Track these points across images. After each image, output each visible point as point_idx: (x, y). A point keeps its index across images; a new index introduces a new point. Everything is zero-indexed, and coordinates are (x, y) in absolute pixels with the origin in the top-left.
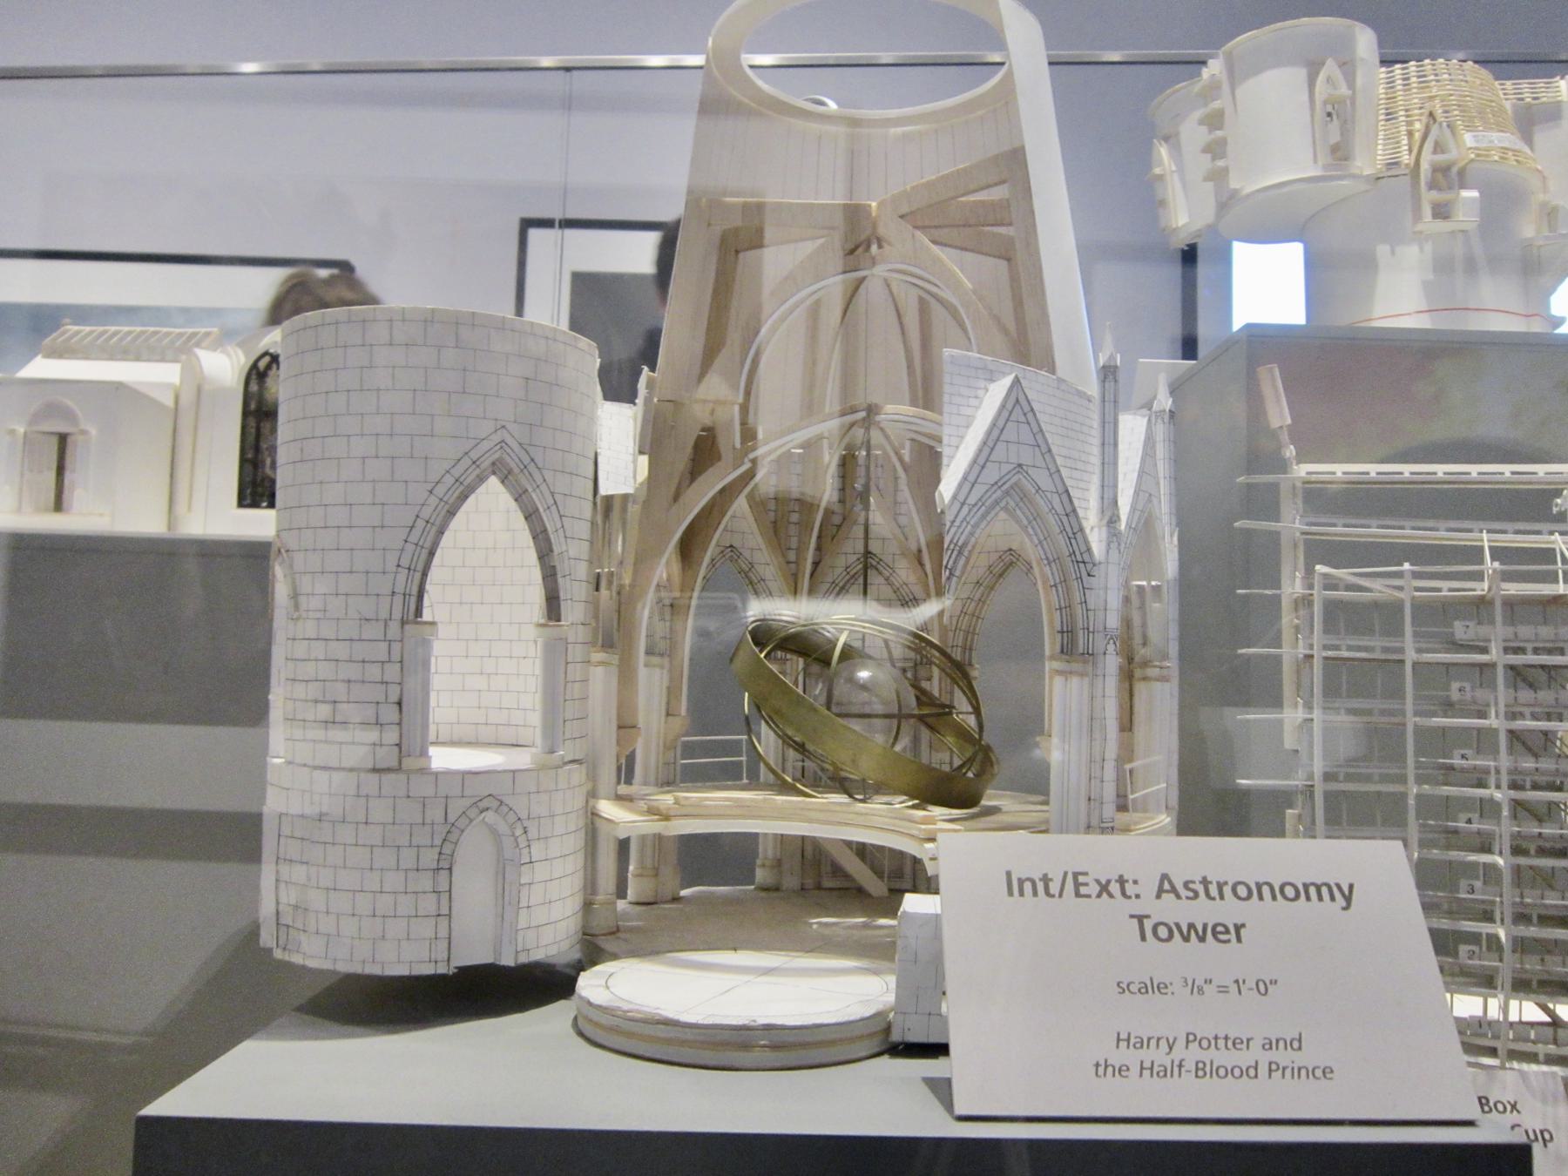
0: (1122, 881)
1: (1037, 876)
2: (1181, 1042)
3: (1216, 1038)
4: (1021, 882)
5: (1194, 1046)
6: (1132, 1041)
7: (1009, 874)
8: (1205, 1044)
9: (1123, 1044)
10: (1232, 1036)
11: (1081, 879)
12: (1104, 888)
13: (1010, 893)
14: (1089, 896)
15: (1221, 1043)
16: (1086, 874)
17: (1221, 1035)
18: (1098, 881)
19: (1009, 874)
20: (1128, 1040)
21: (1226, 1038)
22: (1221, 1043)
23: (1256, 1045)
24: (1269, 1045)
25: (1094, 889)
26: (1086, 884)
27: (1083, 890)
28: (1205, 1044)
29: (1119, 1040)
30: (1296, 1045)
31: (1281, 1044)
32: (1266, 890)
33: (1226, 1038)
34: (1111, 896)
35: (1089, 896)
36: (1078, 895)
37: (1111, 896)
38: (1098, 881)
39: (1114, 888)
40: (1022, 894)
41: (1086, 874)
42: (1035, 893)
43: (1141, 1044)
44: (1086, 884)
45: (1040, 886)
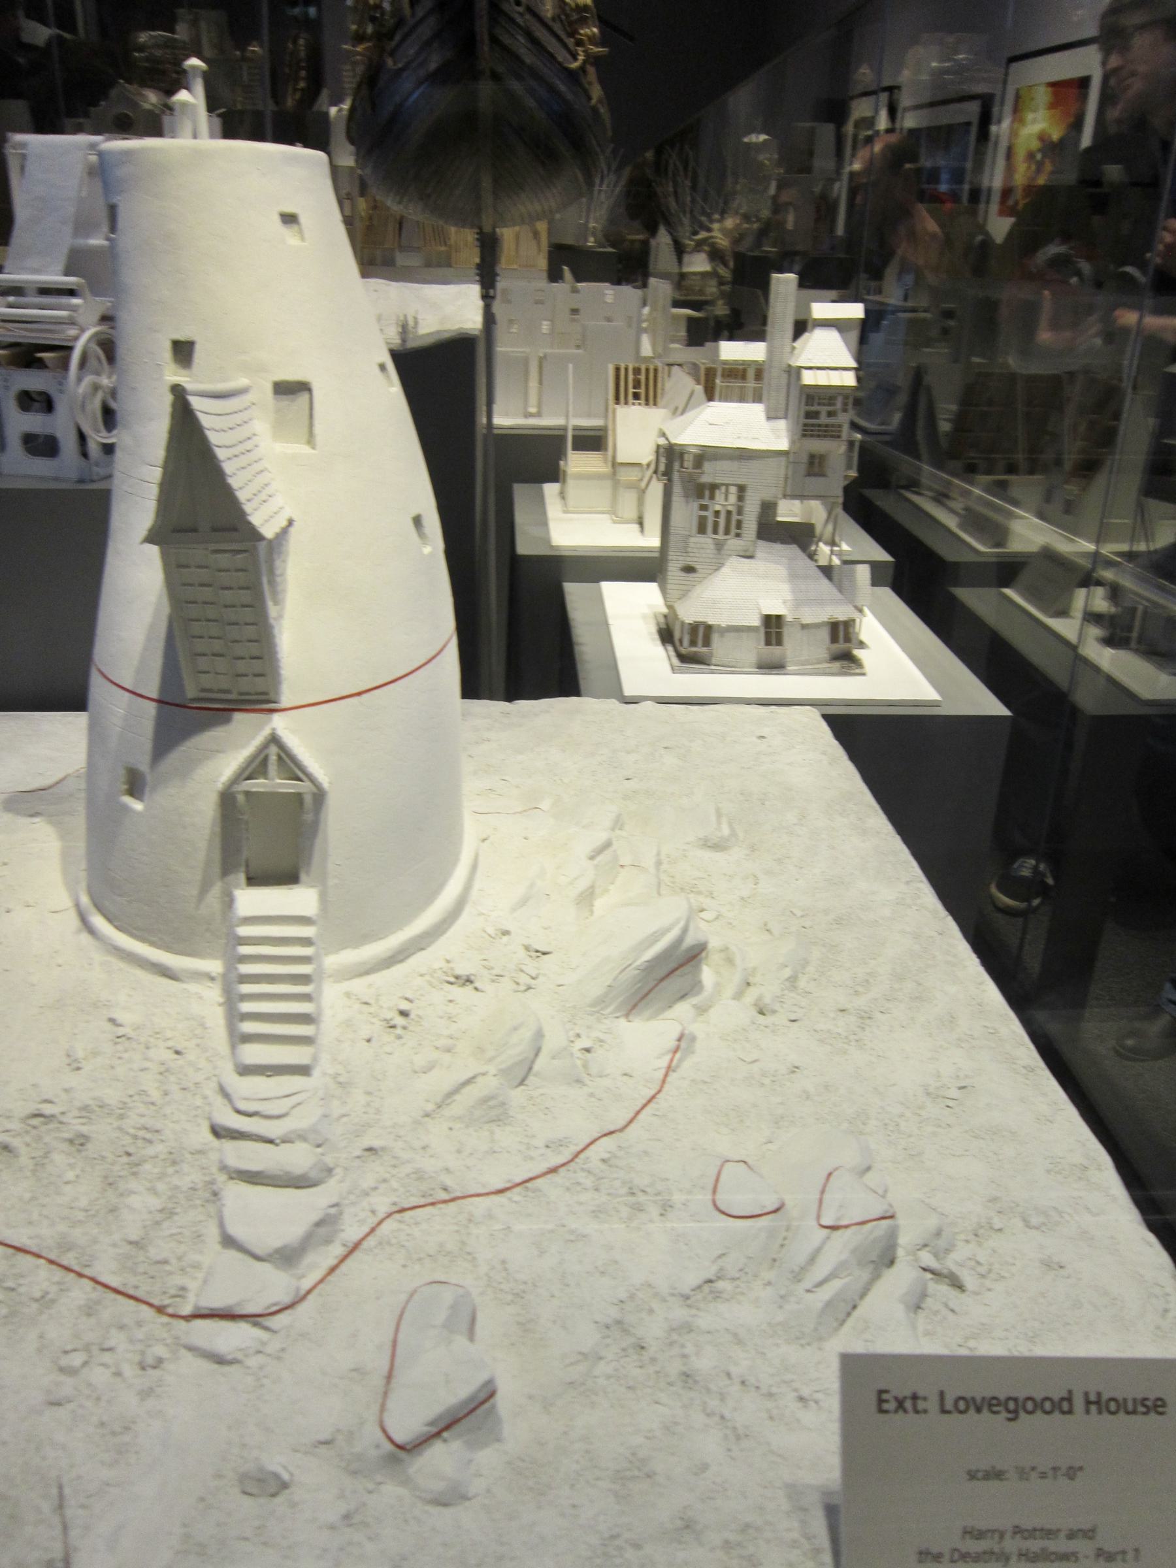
0: (915, 1397)
11: (885, 1396)
12: (900, 1404)
14: (886, 1412)
16: (887, 1392)
18: (896, 1399)
23: (1062, 1535)
24: (1071, 1535)
25: (891, 1406)
26: (887, 1401)
27: (886, 1406)
34: (905, 1411)
35: (886, 1412)
36: (881, 1411)
37: (905, 1411)
38: (896, 1399)
39: (908, 1404)
41: (887, 1392)
44: (887, 1401)
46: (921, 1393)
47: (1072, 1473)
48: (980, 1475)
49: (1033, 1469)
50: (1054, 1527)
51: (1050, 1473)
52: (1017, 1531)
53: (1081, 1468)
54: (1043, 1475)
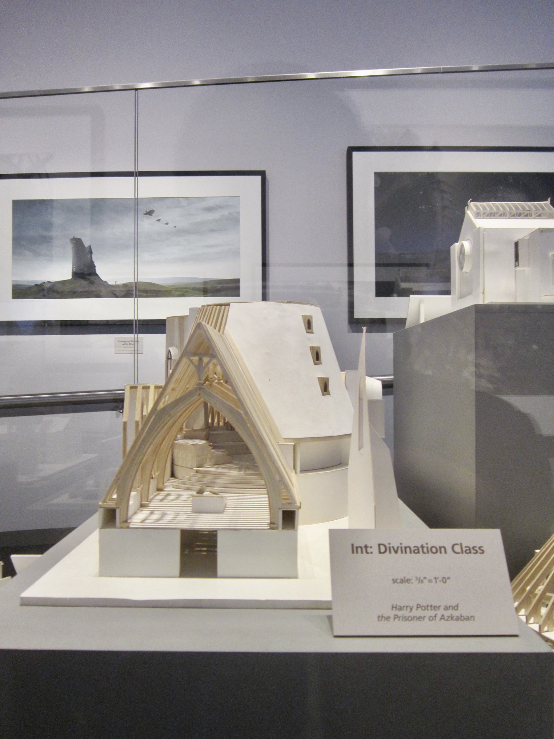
1: (363, 546)
2: (415, 608)
3: (428, 606)
4: (357, 548)
5: (419, 609)
6: (398, 607)
7: (353, 545)
8: (423, 608)
9: (394, 609)
10: (434, 605)
13: (353, 552)
15: (429, 608)
17: (430, 605)
19: (353, 545)
20: (396, 607)
21: (431, 606)
22: (429, 608)
23: (442, 609)
24: (446, 608)
28: (423, 608)
29: (393, 607)
30: (456, 608)
31: (451, 608)
32: (443, 550)
33: (431, 606)
40: (357, 552)
42: (362, 552)
43: (401, 609)
45: (364, 550)
46: (368, 545)
47: (445, 580)
48: (398, 581)
49: (425, 578)
50: (438, 605)
51: (434, 580)
52: (418, 606)
53: (449, 578)
54: (430, 581)
